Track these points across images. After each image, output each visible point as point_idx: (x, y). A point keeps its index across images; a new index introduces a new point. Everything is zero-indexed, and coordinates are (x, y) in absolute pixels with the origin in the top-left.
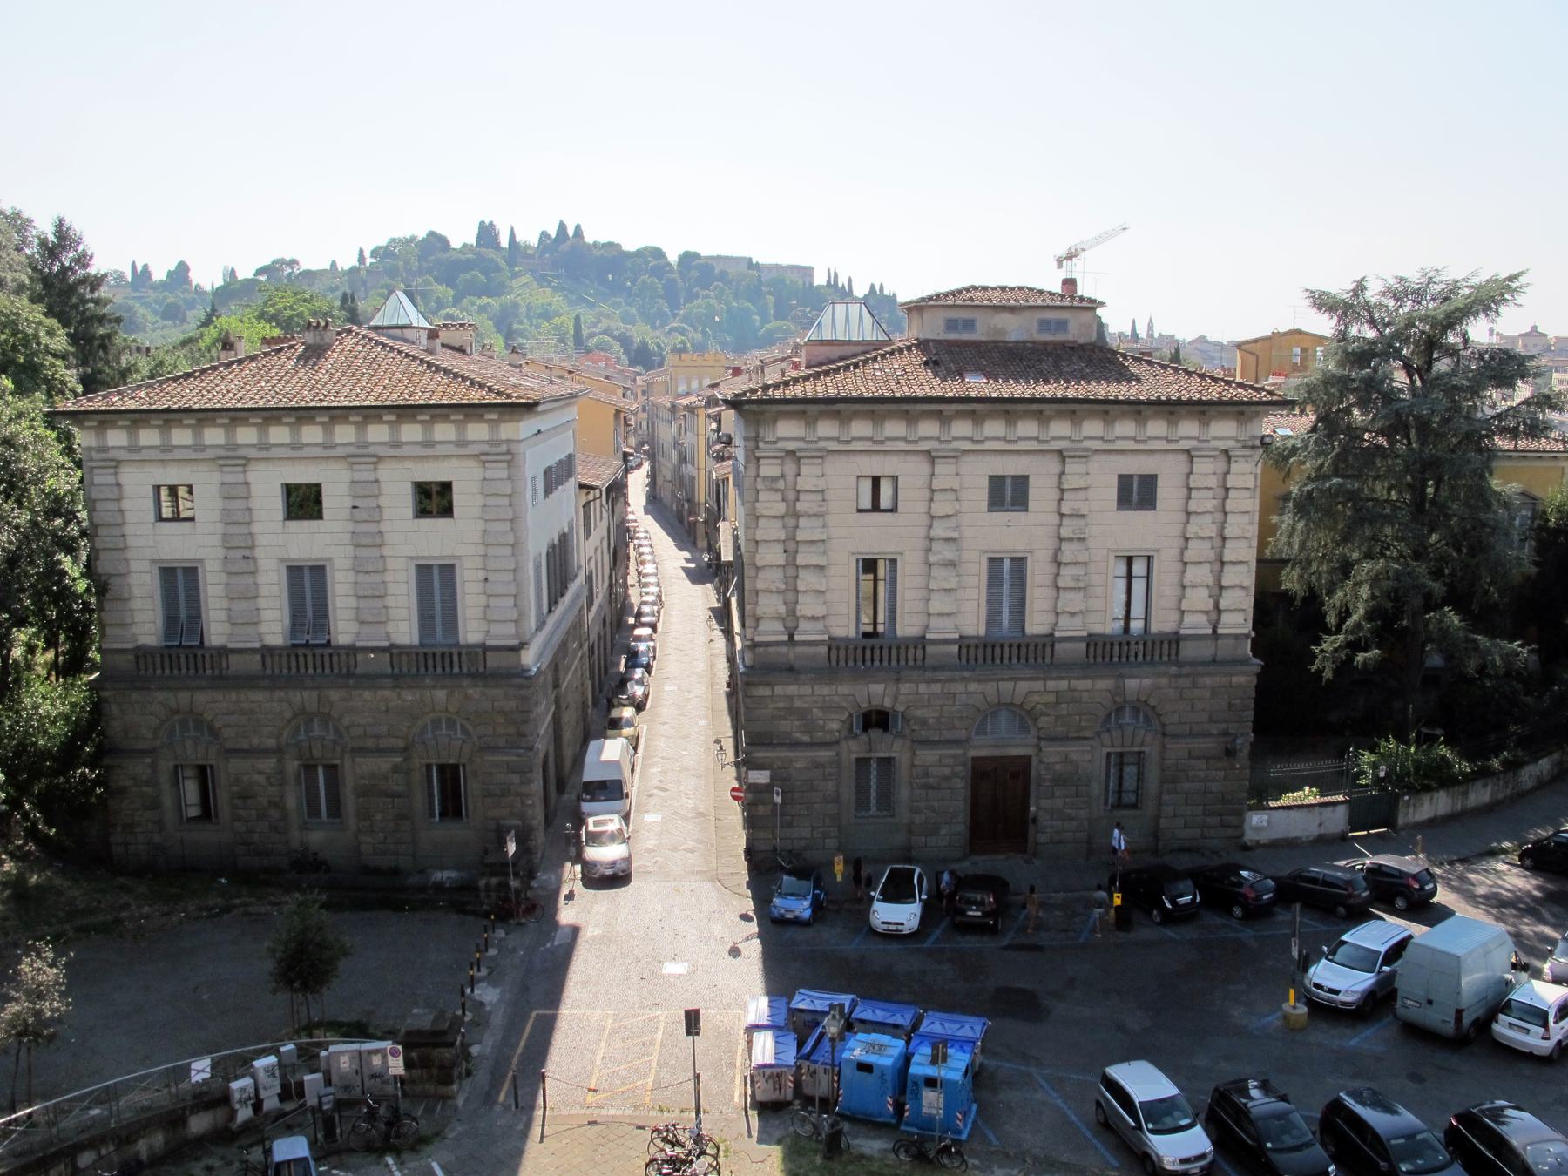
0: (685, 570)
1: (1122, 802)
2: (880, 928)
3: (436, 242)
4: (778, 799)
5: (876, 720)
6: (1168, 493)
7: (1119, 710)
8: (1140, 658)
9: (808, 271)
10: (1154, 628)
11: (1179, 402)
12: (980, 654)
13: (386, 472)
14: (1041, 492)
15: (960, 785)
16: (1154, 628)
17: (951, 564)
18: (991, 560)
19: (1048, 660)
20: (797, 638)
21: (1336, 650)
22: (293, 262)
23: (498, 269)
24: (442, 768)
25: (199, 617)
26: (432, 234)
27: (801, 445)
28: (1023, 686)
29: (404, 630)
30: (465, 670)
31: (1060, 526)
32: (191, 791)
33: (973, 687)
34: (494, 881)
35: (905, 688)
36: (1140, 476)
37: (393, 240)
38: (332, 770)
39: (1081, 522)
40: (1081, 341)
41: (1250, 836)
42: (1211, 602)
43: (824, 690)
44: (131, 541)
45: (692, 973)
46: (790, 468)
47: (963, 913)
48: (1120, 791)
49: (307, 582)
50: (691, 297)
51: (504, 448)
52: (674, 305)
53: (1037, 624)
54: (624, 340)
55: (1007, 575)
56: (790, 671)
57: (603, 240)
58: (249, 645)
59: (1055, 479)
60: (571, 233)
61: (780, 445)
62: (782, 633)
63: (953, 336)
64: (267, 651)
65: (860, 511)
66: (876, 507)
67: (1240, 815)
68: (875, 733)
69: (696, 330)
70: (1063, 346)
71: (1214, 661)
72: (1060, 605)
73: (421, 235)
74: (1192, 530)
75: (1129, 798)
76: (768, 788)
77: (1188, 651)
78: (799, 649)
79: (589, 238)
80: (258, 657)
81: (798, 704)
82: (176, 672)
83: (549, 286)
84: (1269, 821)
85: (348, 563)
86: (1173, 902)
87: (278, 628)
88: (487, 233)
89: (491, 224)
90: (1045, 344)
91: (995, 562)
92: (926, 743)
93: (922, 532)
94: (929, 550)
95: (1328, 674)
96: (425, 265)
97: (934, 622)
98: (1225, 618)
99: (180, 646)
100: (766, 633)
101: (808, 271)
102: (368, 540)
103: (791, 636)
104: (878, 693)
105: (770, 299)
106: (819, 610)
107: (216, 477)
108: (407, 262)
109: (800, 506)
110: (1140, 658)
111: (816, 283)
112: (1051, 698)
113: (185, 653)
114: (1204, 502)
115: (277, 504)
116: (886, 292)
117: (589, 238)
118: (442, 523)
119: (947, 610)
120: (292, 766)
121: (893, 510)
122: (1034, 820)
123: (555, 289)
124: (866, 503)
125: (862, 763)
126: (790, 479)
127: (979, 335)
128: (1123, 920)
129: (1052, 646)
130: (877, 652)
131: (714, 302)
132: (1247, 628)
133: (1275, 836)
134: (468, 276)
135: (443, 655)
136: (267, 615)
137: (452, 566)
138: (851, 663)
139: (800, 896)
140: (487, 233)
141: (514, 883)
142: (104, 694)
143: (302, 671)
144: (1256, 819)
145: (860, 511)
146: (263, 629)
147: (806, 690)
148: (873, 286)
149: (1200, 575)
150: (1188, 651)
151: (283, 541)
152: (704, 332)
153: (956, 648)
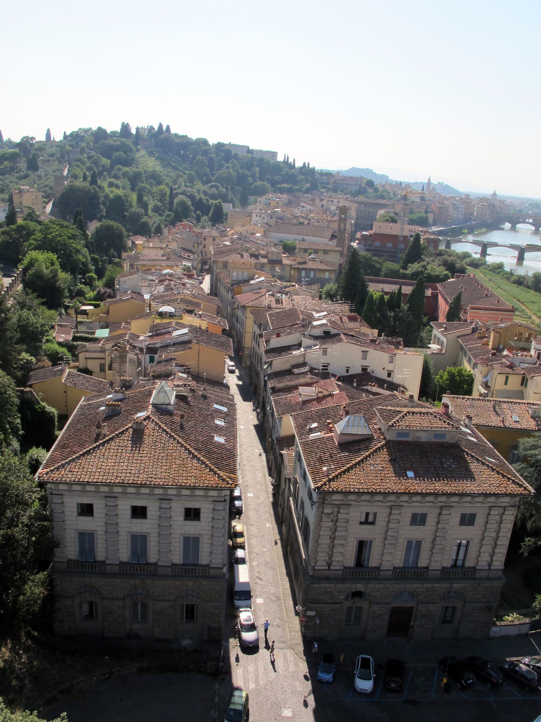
0: (238, 385)
1: (446, 620)
2: (359, 690)
3: (100, 134)
4: (318, 622)
5: (358, 594)
6: (479, 521)
7: (449, 592)
8: (460, 576)
9: (274, 154)
10: (467, 565)
11: (490, 494)
12: (401, 574)
13: (173, 504)
14: (431, 520)
15: (387, 617)
16: (467, 565)
17: (394, 544)
18: (408, 541)
19: (425, 577)
20: (331, 568)
21: (529, 546)
22: (33, 138)
23: (131, 150)
24: (187, 605)
25: (94, 549)
26: (100, 129)
27: (341, 502)
28: (415, 586)
29: (178, 558)
30: (201, 574)
31: (436, 531)
32: (86, 608)
33: (395, 586)
34: (214, 663)
35: (370, 586)
36: (469, 514)
37: (80, 129)
38: (145, 606)
39: (445, 531)
40: (450, 442)
41: (492, 634)
42: (490, 558)
43: (340, 586)
44: (66, 518)
45: (294, 715)
46: (336, 510)
47: (389, 685)
48: (445, 616)
49: (139, 542)
50: (220, 167)
51: (223, 499)
52: (212, 169)
53: (422, 563)
54: (192, 197)
55: (414, 547)
56: (328, 579)
57: (181, 134)
58: (115, 563)
59: (437, 515)
60: (164, 128)
61: (333, 502)
62: (324, 566)
63: (400, 439)
64: (122, 563)
65: (361, 523)
66: (366, 522)
67: (489, 628)
68: (357, 599)
69: (223, 187)
70: (442, 445)
71: (488, 578)
72: (432, 558)
73: (95, 128)
74: (486, 534)
75: (448, 619)
76: (314, 617)
77: (478, 575)
78: (332, 572)
79: (173, 131)
80: (118, 567)
81: (329, 590)
82: (84, 570)
83: (154, 156)
84: (500, 630)
85: (156, 535)
86: (466, 682)
87: (126, 555)
88: (125, 128)
89: (128, 124)
90: (435, 442)
91: (409, 543)
92: (377, 603)
93: (384, 532)
94: (385, 539)
95: (526, 554)
96: (96, 145)
97: (384, 563)
98: (494, 563)
99: (86, 561)
100: (320, 566)
101: (274, 154)
102: (165, 527)
103: (329, 566)
104: (360, 587)
105: (257, 169)
106: (340, 559)
107: (103, 502)
108: (88, 144)
109: (338, 524)
110: (460, 576)
111: (278, 160)
112: (425, 590)
113: (88, 564)
114: (492, 526)
115: (129, 512)
116: (311, 167)
117: (173, 131)
118: (195, 523)
119: (390, 559)
120: (129, 602)
121: (373, 523)
122: (412, 627)
123: (157, 159)
124: (363, 520)
125: (350, 608)
126: (335, 513)
127: (410, 439)
128: (448, 688)
129: (427, 572)
130: (361, 573)
131: (231, 170)
132: (502, 567)
133: (501, 634)
134: (117, 154)
135: (192, 569)
136: (121, 551)
137: (198, 538)
138: (351, 577)
139: (328, 672)
140: (125, 128)
141: (221, 664)
142: (54, 576)
143: (135, 572)
144: (495, 629)
145: (361, 523)
146: (120, 555)
147: (333, 585)
148: (304, 164)
149: (487, 549)
150: (478, 575)
151: (129, 526)
152: (227, 188)
153: (391, 572)
